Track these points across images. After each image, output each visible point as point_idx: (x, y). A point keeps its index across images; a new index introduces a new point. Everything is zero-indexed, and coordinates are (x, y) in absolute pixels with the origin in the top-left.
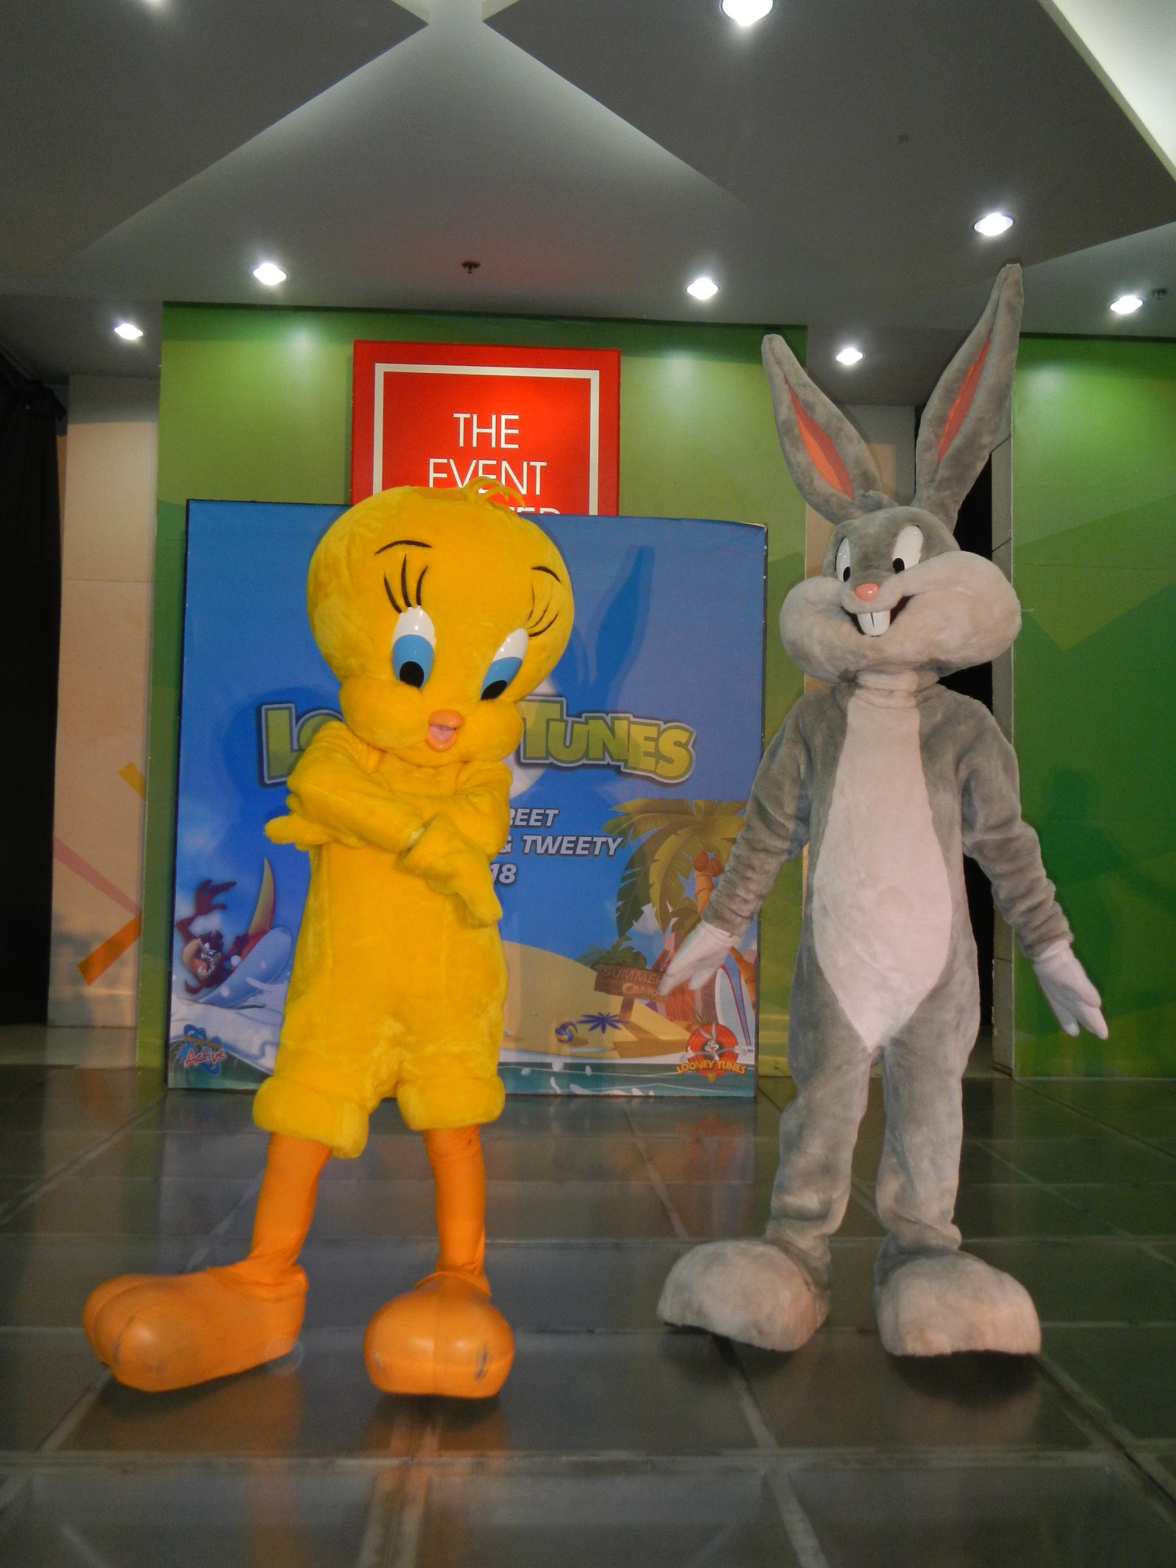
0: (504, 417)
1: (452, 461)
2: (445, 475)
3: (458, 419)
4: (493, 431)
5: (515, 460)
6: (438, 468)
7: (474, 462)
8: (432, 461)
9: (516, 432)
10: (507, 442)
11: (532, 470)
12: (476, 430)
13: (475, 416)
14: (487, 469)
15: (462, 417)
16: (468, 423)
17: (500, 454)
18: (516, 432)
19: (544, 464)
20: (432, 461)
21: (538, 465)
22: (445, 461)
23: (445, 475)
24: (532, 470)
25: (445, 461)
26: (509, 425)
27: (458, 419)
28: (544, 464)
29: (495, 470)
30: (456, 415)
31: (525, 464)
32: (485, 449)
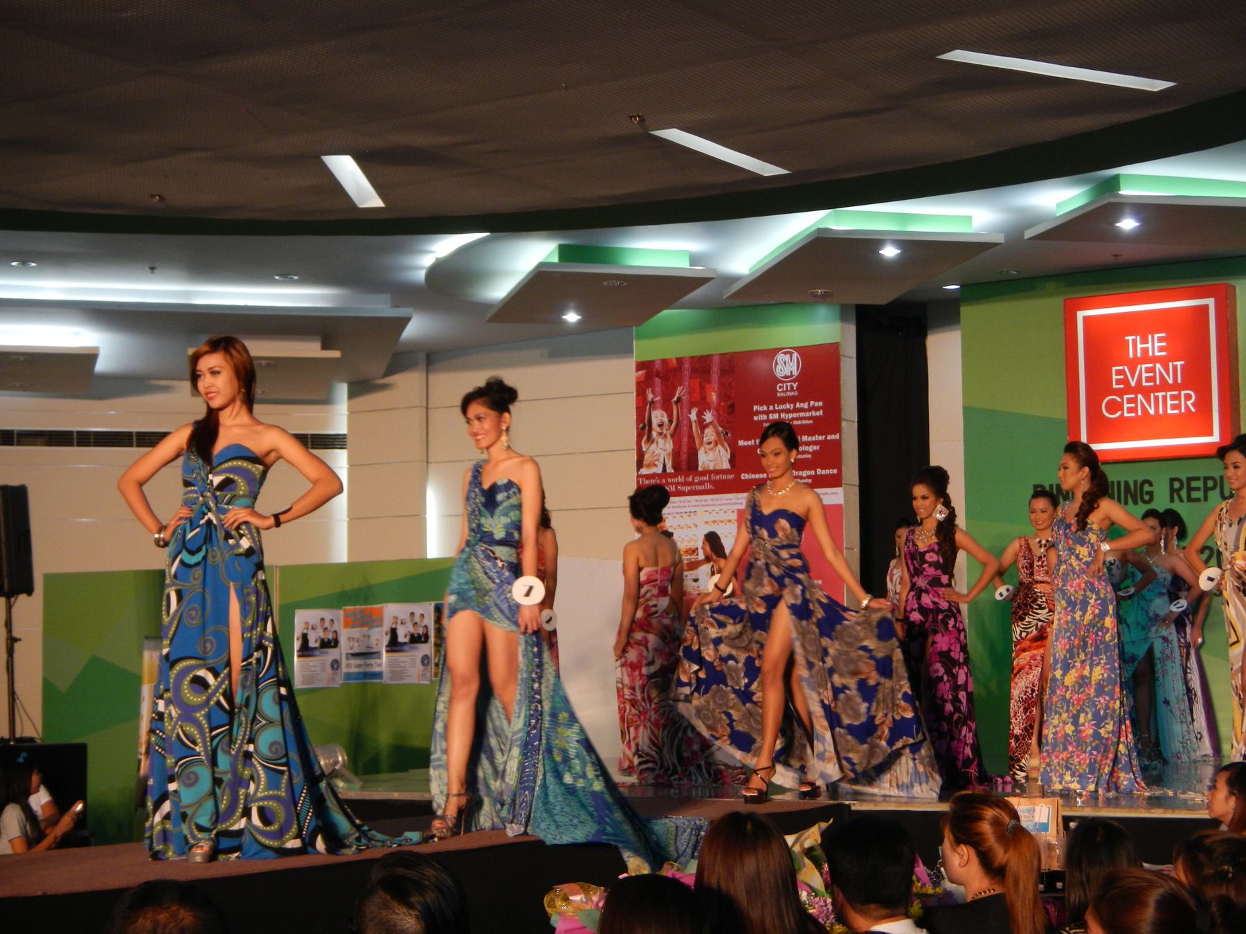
0: (1156, 336)
1: (1126, 368)
2: (1122, 377)
3: (1128, 340)
4: (1149, 345)
5: (1164, 362)
6: (1118, 373)
7: (1139, 366)
8: (1114, 369)
9: (1164, 344)
10: (1146, 382)
11: (1175, 368)
12: (1139, 346)
13: (1138, 337)
14: (1148, 370)
15: (1130, 338)
16: (1135, 342)
17: (1155, 360)
18: (1164, 344)
19: (1182, 363)
20: (1114, 369)
21: (1179, 364)
22: (1121, 368)
23: (1122, 377)
24: (1175, 368)
25: (1121, 368)
26: (1160, 340)
27: (1128, 340)
28: (1182, 363)
29: (1152, 370)
30: (1127, 338)
31: (1158, 383)
32: (1146, 358)
